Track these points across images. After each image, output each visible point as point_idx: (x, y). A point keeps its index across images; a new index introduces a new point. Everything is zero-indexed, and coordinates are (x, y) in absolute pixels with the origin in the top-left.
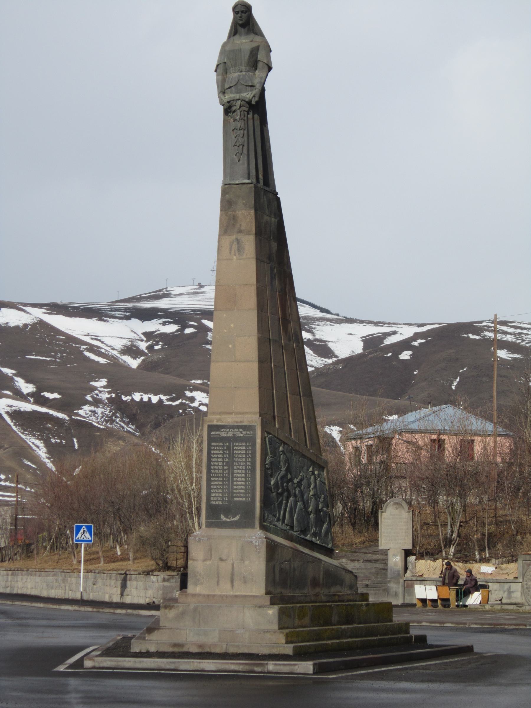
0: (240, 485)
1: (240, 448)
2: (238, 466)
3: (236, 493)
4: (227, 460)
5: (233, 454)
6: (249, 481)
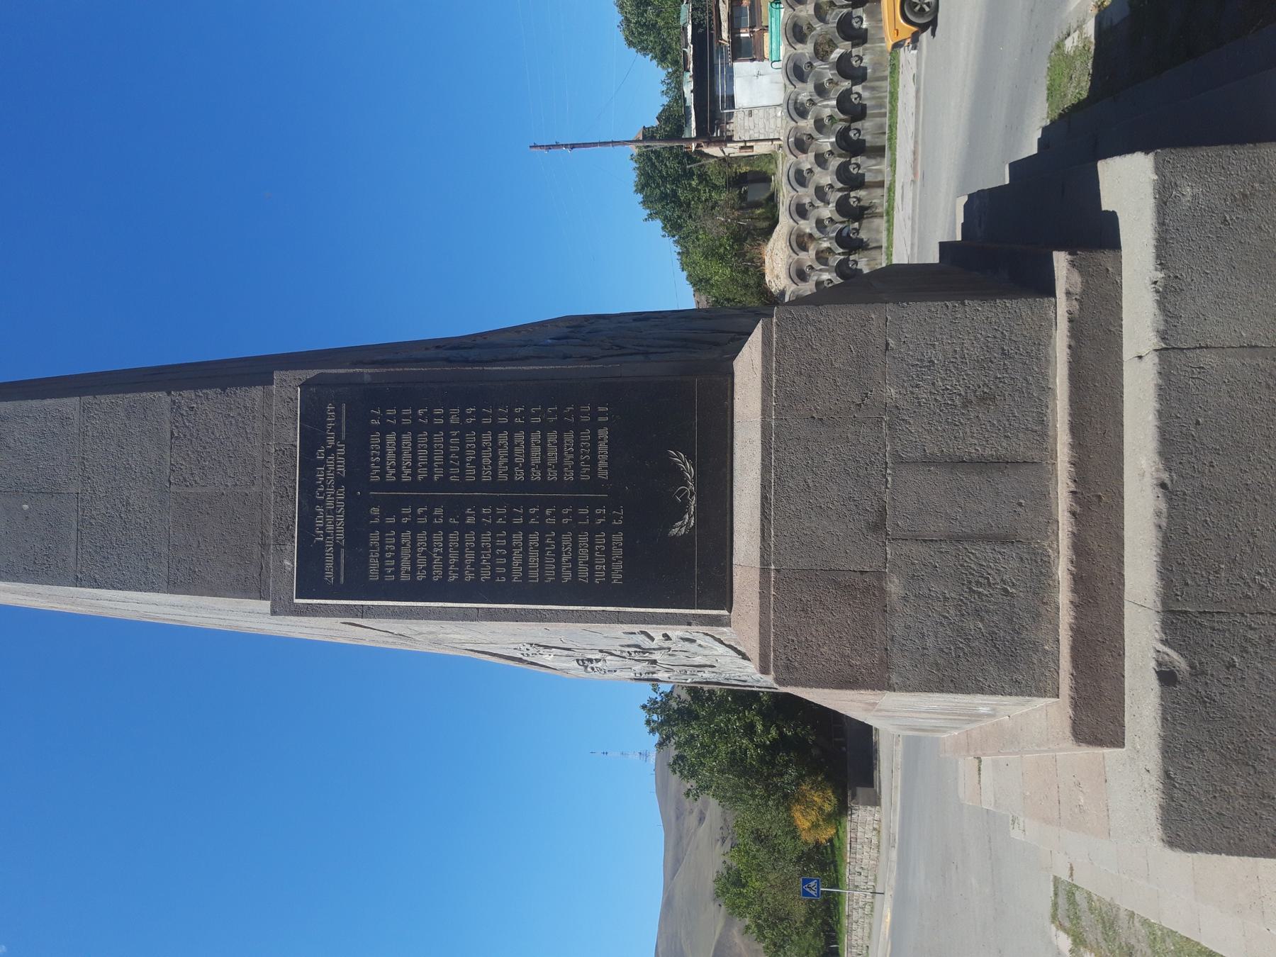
0: (544, 451)
1: (390, 455)
2: (463, 462)
3: (577, 468)
4: (438, 511)
5: (413, 485)
6: (526, 415)
